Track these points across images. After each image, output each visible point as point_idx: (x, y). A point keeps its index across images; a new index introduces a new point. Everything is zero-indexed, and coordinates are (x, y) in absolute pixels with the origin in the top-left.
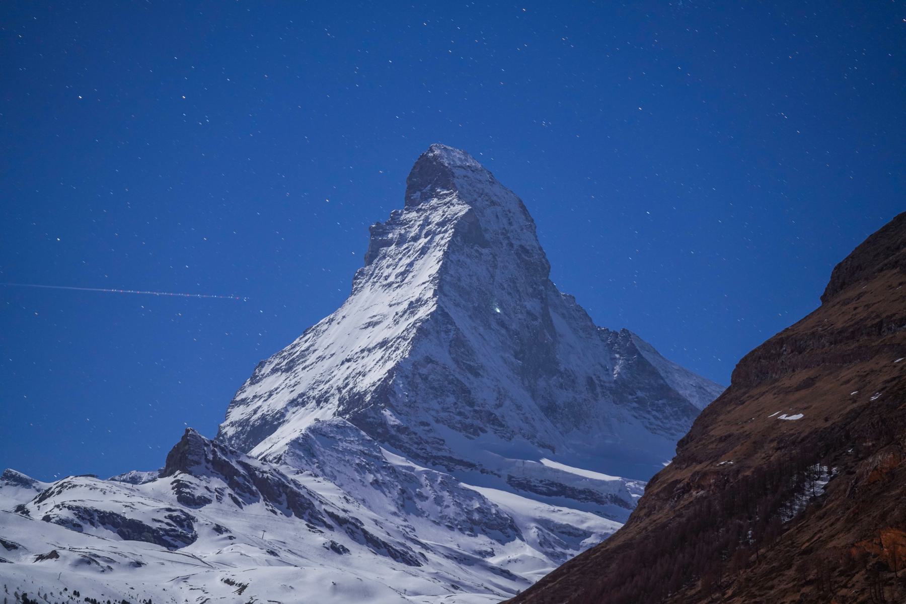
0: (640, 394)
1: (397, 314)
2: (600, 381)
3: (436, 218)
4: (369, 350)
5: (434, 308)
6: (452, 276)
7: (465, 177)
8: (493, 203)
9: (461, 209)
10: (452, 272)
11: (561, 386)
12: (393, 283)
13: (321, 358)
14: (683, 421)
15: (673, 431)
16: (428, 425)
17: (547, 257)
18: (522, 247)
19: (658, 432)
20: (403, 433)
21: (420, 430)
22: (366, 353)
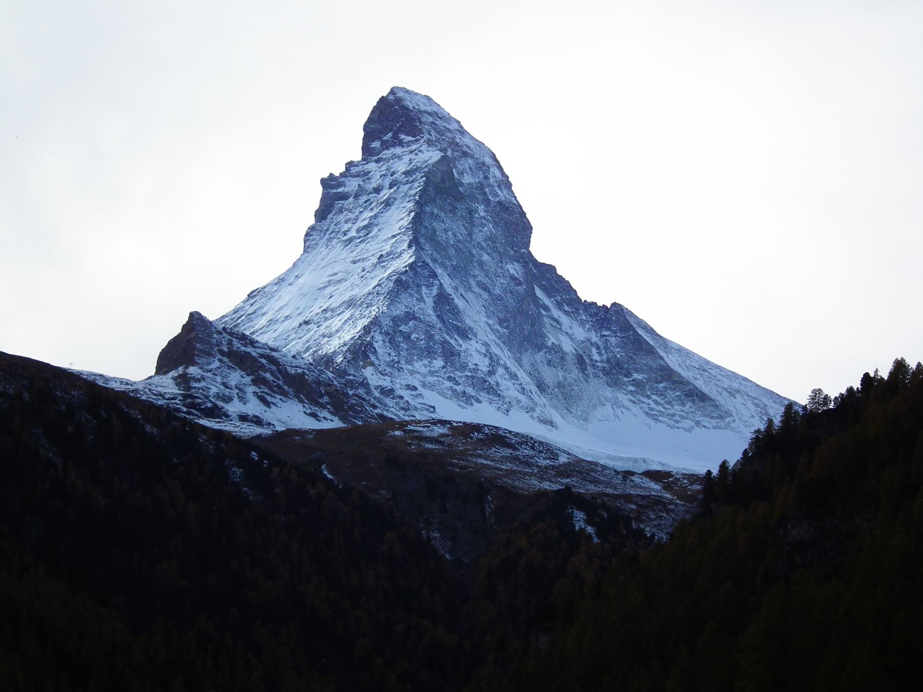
0: (636, 376)
1: (363, 270)
2: (591, 360)
3: (401, 167)
4: (333, 310)
5: (412, 260)
6: (426, 227)
7: (432, 123)
8: (465, 155)
9: (434, 156)
10: (426, 224)
11: (549, 363)
12: (355, 238)
13: (271, 322)
14: (688, 406)
15: (677, 418)
16: (415, 389)
17: (527, 216)
18: (499, 203)
19: (660, 418)
20: (387, 396)
21: (406, 394)
22: (329, 314)
